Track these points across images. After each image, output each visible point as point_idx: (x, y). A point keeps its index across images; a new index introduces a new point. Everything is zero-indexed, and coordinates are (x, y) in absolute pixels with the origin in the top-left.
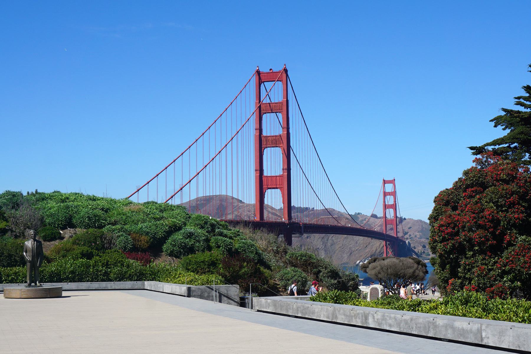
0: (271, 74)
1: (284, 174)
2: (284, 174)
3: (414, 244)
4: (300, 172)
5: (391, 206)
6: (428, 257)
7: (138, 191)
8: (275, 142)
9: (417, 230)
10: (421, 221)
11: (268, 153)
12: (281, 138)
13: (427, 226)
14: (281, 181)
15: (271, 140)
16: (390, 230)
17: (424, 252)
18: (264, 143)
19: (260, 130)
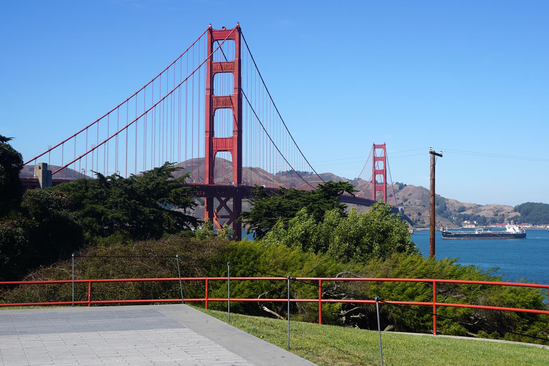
0: (224, 32)
1: (235, 136)
2: (235, 136)
3: (409, 211)
4: (263, 135)
5: (380, 172)
6: (423, 225)
7: (50, 150)
8: (226, 102)
9: (417, 197)
10: (421, 188)
11: (219, 113)
12: (231, 98)
13: (427, 193)
14: (231, 143)
15: (222, 100)
16: (389, 196)
17: (419, 220)
18: (215, 104)
19: (211, 90)
